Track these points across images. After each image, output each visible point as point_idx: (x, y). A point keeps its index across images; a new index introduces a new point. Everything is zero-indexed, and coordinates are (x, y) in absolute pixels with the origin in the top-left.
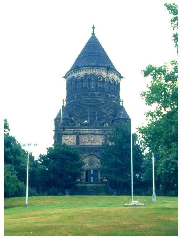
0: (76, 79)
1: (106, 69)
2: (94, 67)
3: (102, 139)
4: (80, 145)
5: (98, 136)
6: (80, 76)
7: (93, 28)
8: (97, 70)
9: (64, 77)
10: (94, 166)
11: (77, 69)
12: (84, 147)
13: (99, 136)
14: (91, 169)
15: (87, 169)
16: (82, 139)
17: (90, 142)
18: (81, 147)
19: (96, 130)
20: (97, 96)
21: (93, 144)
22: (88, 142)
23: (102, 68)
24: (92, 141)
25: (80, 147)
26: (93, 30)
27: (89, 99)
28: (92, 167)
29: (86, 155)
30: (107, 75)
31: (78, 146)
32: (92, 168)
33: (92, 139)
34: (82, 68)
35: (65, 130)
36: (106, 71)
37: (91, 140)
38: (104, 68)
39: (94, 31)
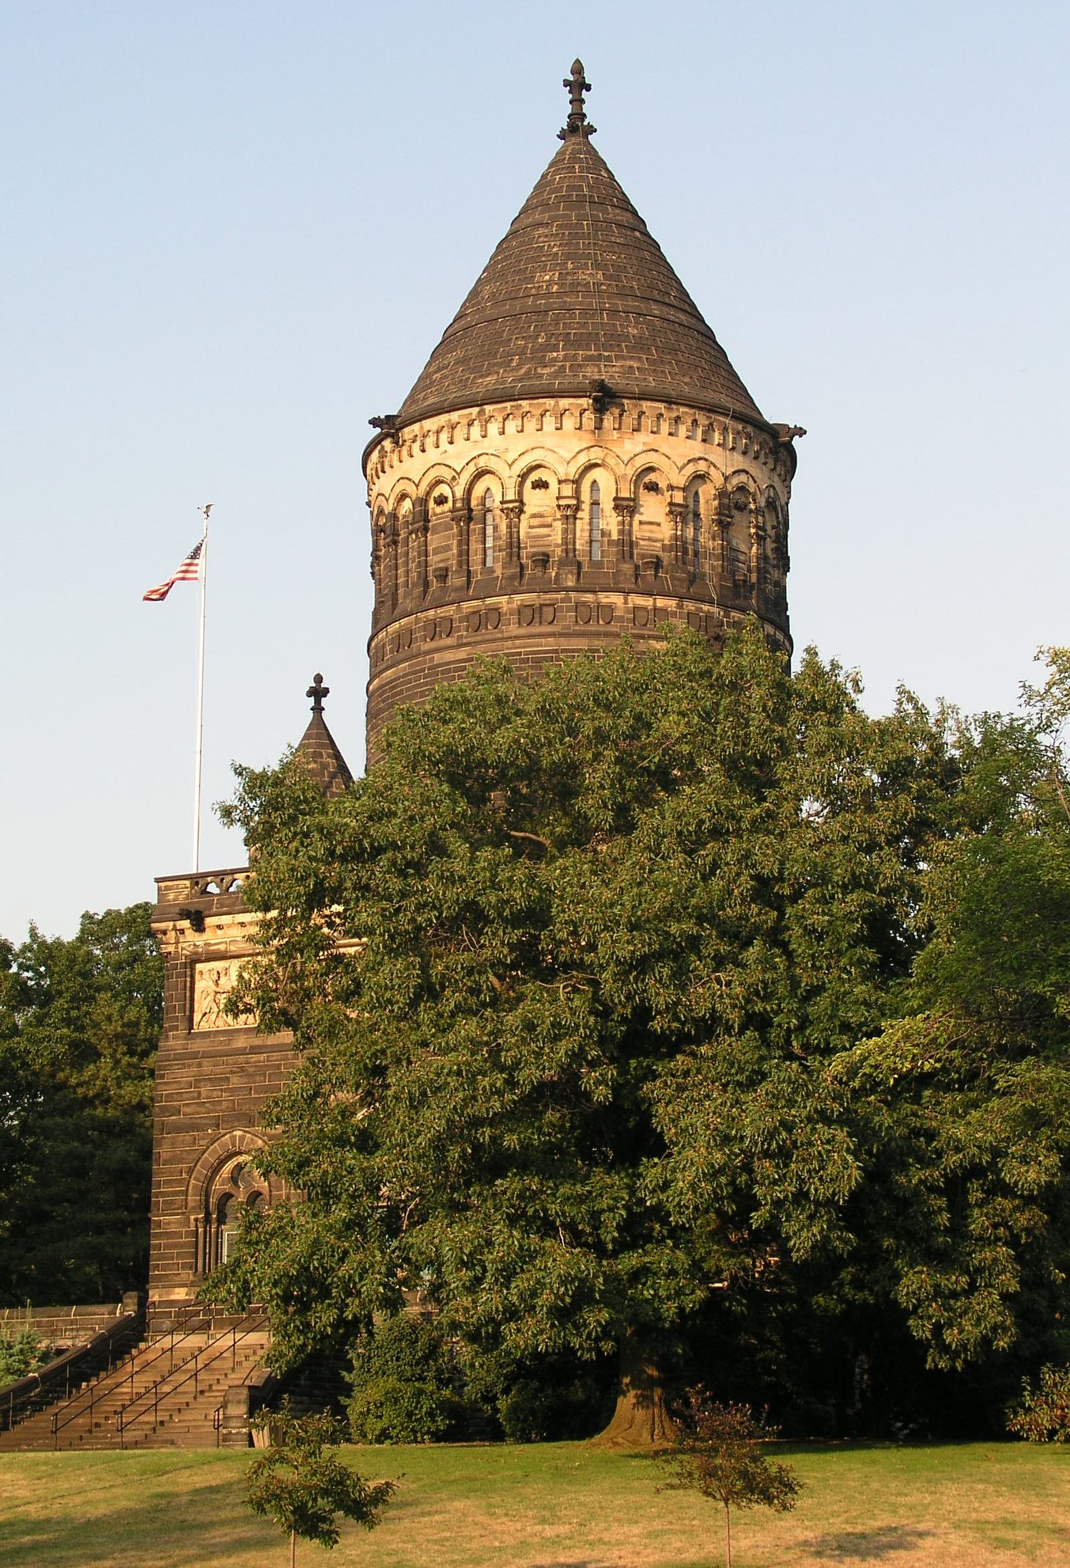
1: (585, 402)
2: (488, 408)
7: (578, 85)
20: (514, 630)
26: (578, 101)
27: (462, 654)
30: (596, 455)
35: (209, 921)
36: (589, 419)
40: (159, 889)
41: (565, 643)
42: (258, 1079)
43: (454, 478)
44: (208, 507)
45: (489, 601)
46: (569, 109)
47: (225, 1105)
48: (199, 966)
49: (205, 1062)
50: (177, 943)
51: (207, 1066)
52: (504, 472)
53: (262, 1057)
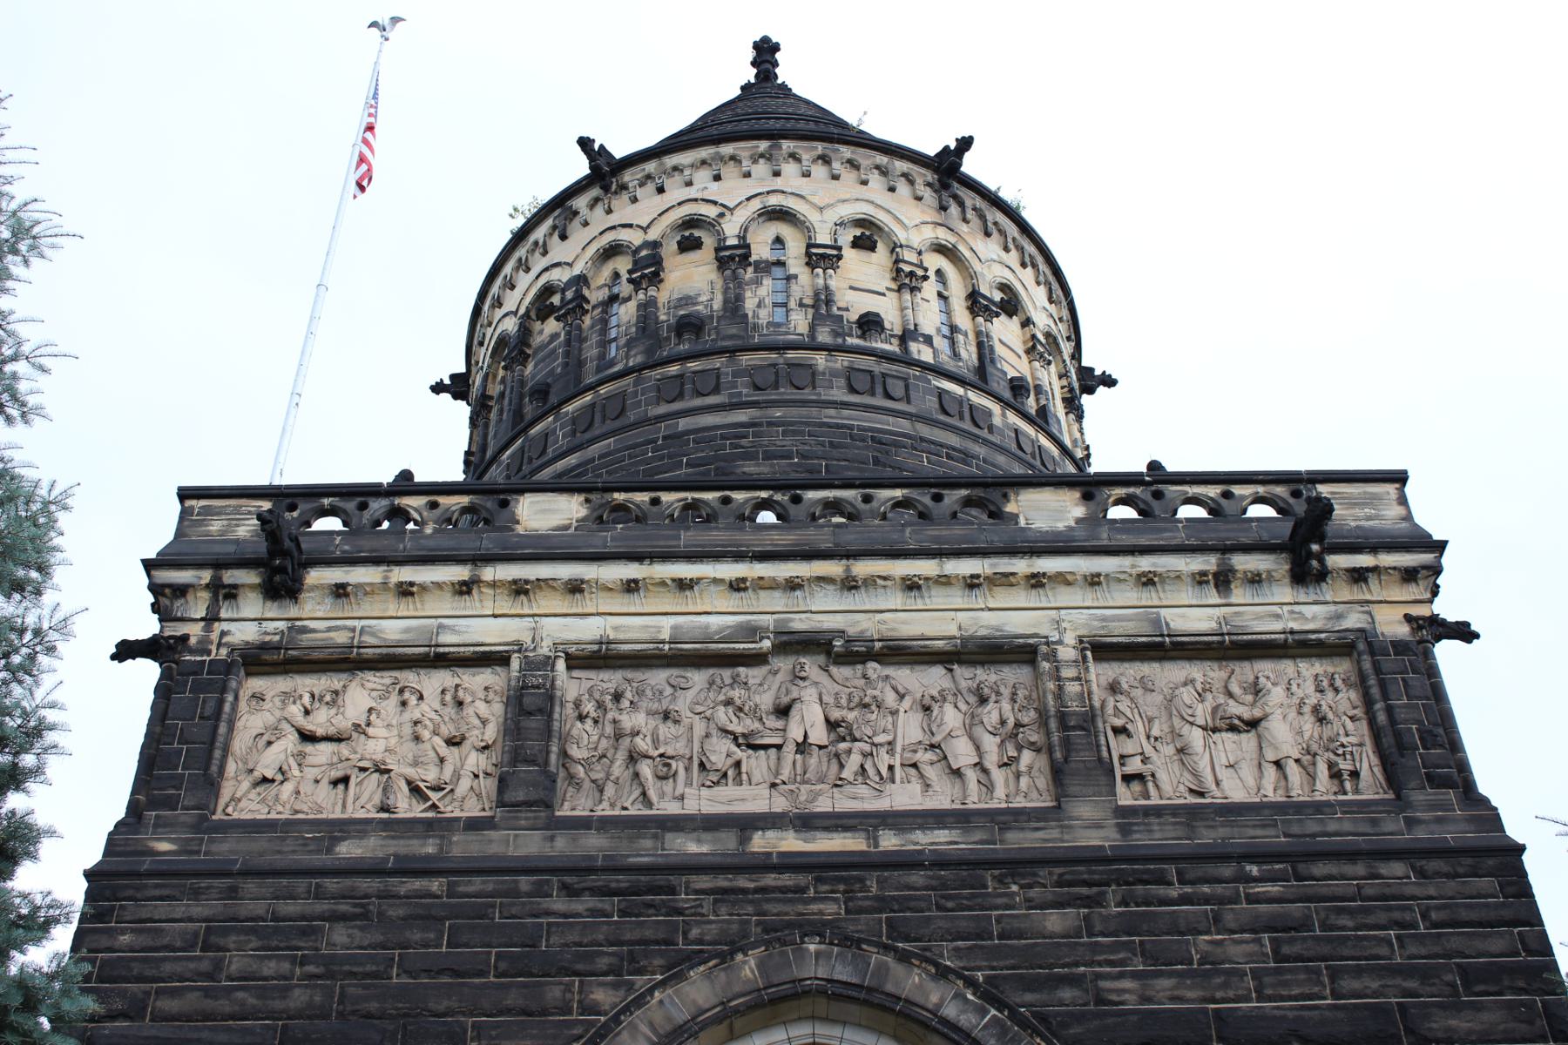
0: (581, 280)
1: (930, 176)
2: (787, 145)
3: (991, 715)
4: (583, 824)
5: (904, 676)
6: (624, 235)
7: (765, 52)
8: (819, 171)
9: (457, 387)
11: (595, 192)
12: (644, 851)
13: (933, 679)
16: (618, 736)
17: (757, 764)
18: (594, 844)
19: (863, 568)
20: (839, 393)
21: (823, 805)
23: (882, 159)
24: (803, 747)
25: (562, 845)
27: (741, 416)
30: (944, 236)
31: (528, 844)
33: (810, 720)
34: (651, 167)
37: (796, 733)
38: (901, 166)
39: (784, 74)
40: (185, 514)
41: (925, 431)
42: (417, 936)
43: (722, 215)
44: (395, 20)
45: (791, 355)
46: (750, 74)
47: (299, 998)
48: (256, 684)
49: (250, 886)
50: (211, 618)
51: (254, 902)
52: (813, 217)
53: (435, 885)
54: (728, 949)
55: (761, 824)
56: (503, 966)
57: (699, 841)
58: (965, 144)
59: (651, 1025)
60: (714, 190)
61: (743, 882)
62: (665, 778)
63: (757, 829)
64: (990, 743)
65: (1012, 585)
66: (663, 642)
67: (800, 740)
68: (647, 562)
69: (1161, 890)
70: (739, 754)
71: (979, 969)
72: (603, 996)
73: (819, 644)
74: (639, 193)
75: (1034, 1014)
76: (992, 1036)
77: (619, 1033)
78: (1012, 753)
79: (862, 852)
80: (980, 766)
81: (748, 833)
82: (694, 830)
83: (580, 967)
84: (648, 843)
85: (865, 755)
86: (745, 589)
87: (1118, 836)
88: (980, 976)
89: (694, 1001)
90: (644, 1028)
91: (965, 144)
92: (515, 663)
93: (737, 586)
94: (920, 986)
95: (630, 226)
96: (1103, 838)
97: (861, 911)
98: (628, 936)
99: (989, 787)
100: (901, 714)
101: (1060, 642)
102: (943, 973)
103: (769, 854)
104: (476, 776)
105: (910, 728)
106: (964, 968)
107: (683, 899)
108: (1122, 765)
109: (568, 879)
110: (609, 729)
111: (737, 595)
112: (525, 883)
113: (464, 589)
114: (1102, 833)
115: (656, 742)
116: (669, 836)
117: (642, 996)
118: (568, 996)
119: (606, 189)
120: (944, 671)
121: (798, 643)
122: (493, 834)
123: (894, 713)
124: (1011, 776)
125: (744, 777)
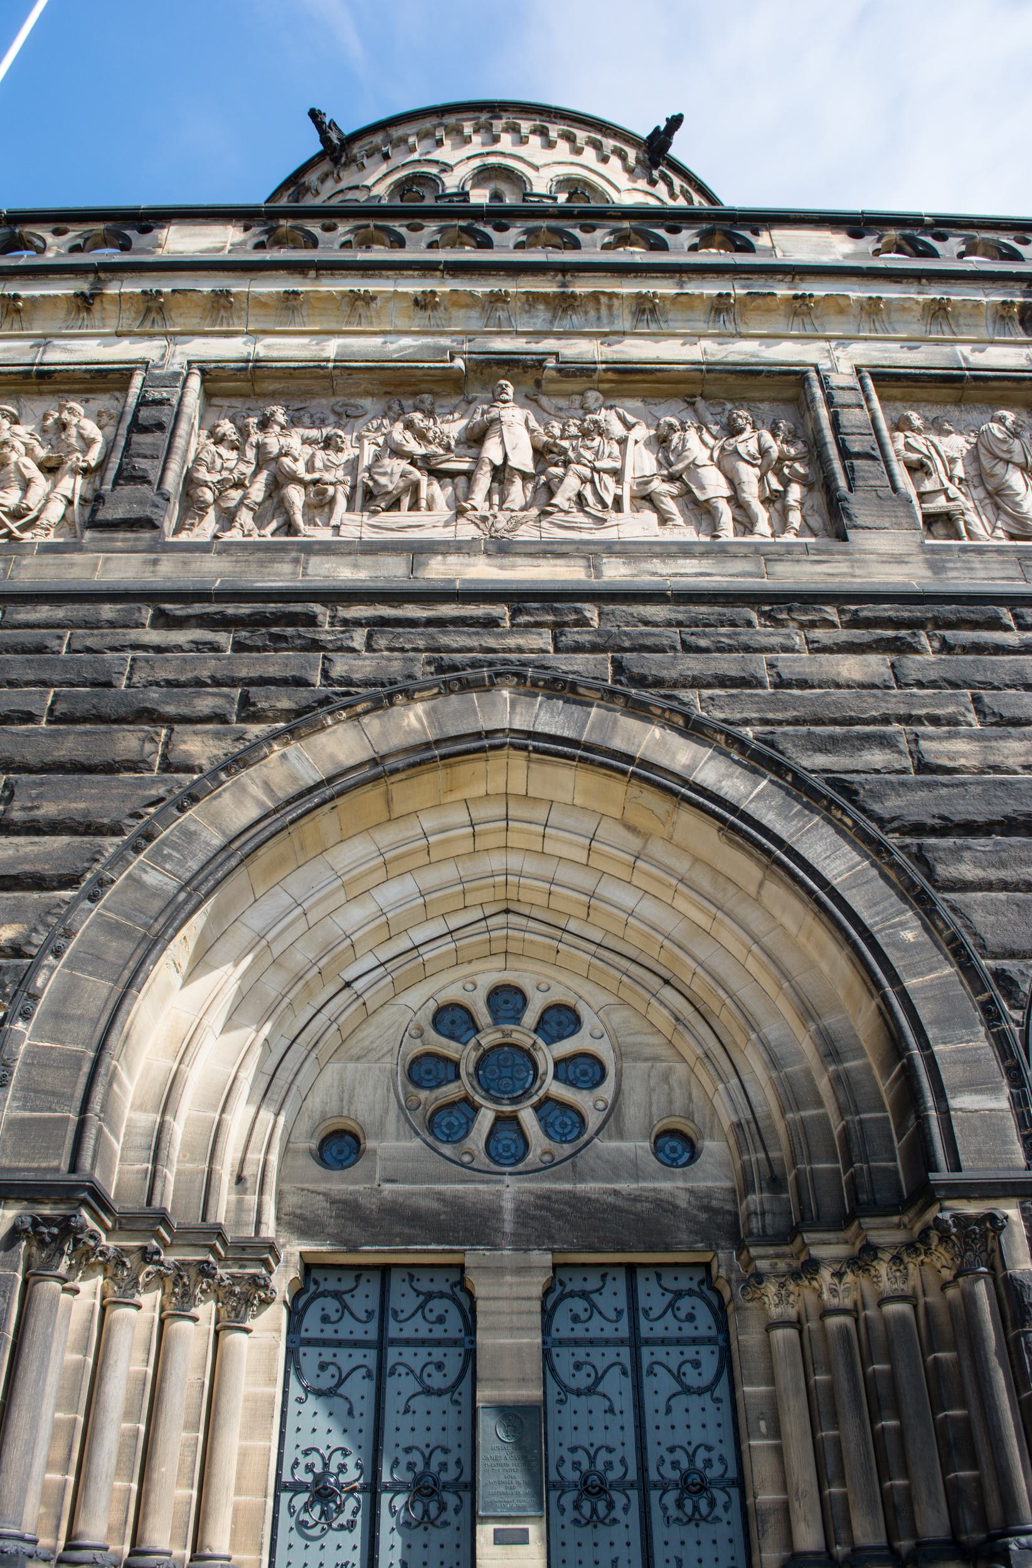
3: (747, 443)
10: (562, 1120)
11: (325, 166)
14: (472, 1225)
15: (349, 1210)
21: (527, 533)
22: (395, 505)
25: (167, 572)
28: (507, 1144)
29: (340, 744)
31: (120, 566)
32: (510, 1191)
34: (378, 139)
54: (386, 694)
55: (442, 548)
56: (61, 708)
57: (356, 566)
58: (675, 122)
59: (267, 786)
60: (437, 155)
61: (412, 611)
62: (320, 506)
63: (436, 553)
64: (749, 475)
65: (769, 310)
66: (328, 361)
67: (498, 461)
68: (312, 274)
69: (997, 637)
70: (417, 474)
71: (746, 722)
72: (199, 747)
73: (525, 367)
74: (365, 161)
75: (834, 783)
76: (770, 808)
77: (219, 795)
78: (775, 484)
79: (578, 582)
80: (736, 501)
81: (422, 558)
82: (350, 554)
83: (170, 709)
84: (286, 568)
85: (584, 481)
86: (435, 306)
87: (929, 573)
88: (749, 732)
89: (332, 757)
90: (256, 791)
91: (675, 122)
92: (137, 381)
93: (423, 303)
94: (662, 743)
95: (356, 188)
96: (913, 576)
97: (578, 648)
98: (243, 673)
99: (745, 522)
100: (631, 443)
101: (834, 369)
102: (694, 729)
103: (453, 581)
104: (70, 502)
105: (642, 461)
106: (725, 721)
107: (326, 632)
108: (922, 501)
109: (167, 606)
110: (251, 454)
111: (421, 313)
112: (108, 611)
113: (85, 302)
114: (905, 569)
115: (310, 467)
116: (314, 560)
117: (256, 746)
118: (149, 747)
119: (336, 161)
120: (683, 405)
121: (500, 363)
122: (77, 557)
123: (622, 442)
124: (775, 516)
125: (423, 503)
